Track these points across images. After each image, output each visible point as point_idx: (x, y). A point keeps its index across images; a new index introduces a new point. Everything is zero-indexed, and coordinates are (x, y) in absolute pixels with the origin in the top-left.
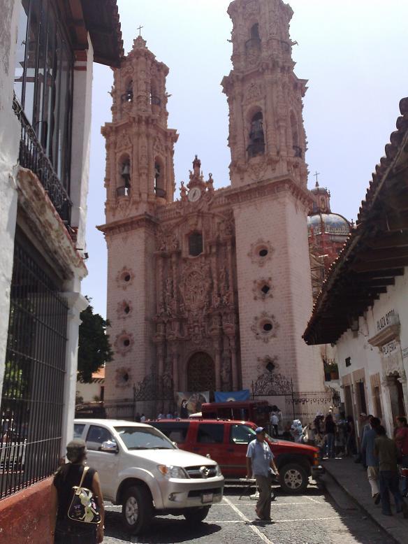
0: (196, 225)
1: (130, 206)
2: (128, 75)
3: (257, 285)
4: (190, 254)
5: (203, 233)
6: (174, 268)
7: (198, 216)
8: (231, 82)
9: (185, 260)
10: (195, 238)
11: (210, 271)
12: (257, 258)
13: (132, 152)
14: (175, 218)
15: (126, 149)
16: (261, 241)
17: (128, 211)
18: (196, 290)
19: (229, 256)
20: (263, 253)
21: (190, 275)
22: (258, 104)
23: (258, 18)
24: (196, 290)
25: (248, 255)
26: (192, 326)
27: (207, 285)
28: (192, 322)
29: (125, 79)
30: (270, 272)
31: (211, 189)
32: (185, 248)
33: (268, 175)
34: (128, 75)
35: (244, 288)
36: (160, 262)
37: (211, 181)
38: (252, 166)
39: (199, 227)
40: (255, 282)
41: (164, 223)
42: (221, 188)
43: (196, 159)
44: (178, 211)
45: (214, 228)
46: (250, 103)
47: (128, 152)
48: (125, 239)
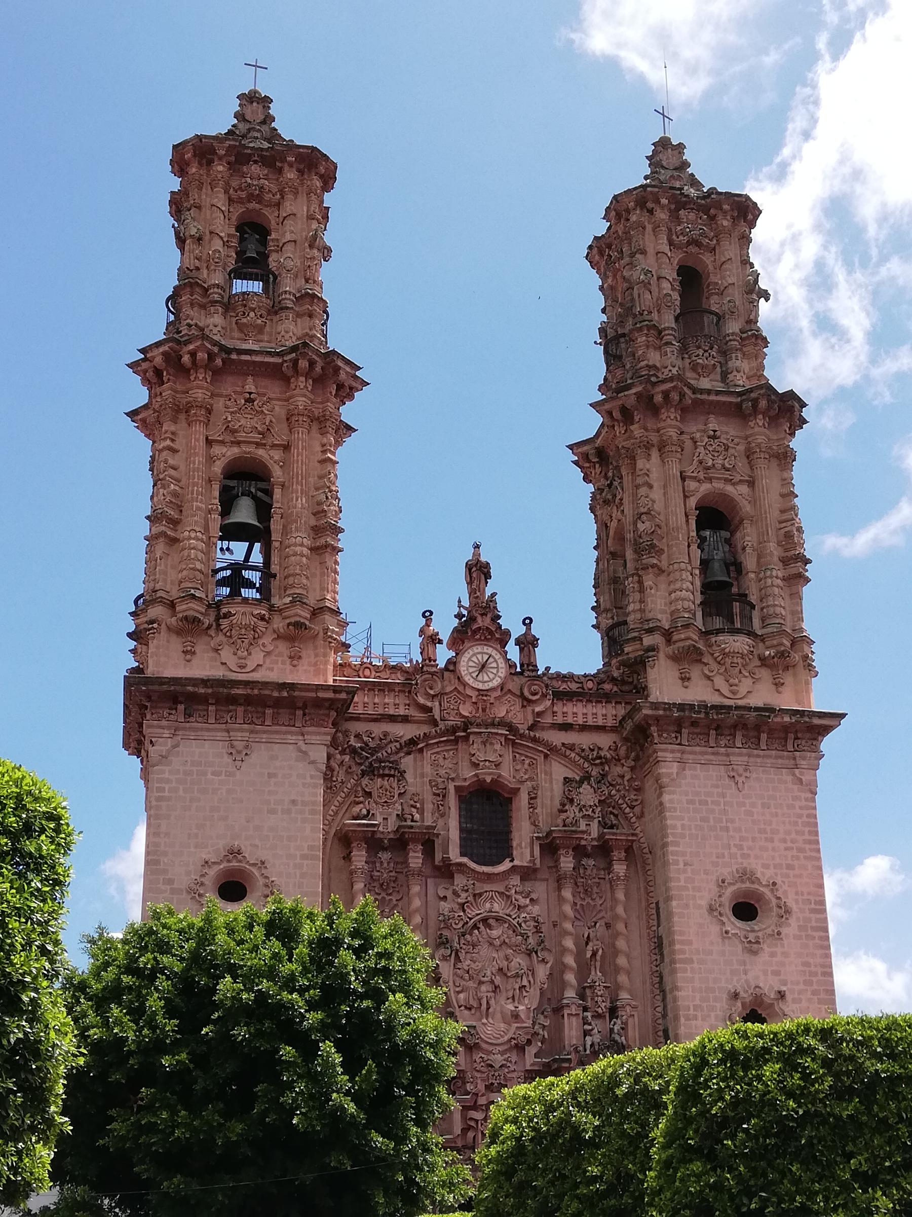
0: (497, 765)
1: (267, 640)
2: (253, 205)
3: (739, 1004)
4: (463, 854)
5: (523, 798)
6: (416, 889)
7: (506, 739)
8: (658, 398)
9: (446, 871)
10: (487, 810)
12: (763, 924)
13: (285, 465)
14: (405, 719)
15: (258, 445)
16: (746, 875)
17: (257, 657)
18: (498, 980)
19: (620, 896)
20: (745, 910)
21: (475, 927)
22: (729, 489)
23: (707, 258)
24: (498, 980)
25: (711, 909)
26: (482, 1101)
27: (542, 972)
28: (481, 1087)
29: (238, 211)
30: (776, 973)
31: (529, 665)
32: (451, 829)
33: (759, 693)
34: (253, 205)
35: (696, 1008)
36: (360, 857)
37: (528, 643)
38: (725, 654)
39: (507, 773)
40: (736, 996)
42: (564, 672)
43: (477, 555)
44: (421, 700)
45: (544, 793)
46: (710, 480)
47: (270, 457)
48: (239, 755)
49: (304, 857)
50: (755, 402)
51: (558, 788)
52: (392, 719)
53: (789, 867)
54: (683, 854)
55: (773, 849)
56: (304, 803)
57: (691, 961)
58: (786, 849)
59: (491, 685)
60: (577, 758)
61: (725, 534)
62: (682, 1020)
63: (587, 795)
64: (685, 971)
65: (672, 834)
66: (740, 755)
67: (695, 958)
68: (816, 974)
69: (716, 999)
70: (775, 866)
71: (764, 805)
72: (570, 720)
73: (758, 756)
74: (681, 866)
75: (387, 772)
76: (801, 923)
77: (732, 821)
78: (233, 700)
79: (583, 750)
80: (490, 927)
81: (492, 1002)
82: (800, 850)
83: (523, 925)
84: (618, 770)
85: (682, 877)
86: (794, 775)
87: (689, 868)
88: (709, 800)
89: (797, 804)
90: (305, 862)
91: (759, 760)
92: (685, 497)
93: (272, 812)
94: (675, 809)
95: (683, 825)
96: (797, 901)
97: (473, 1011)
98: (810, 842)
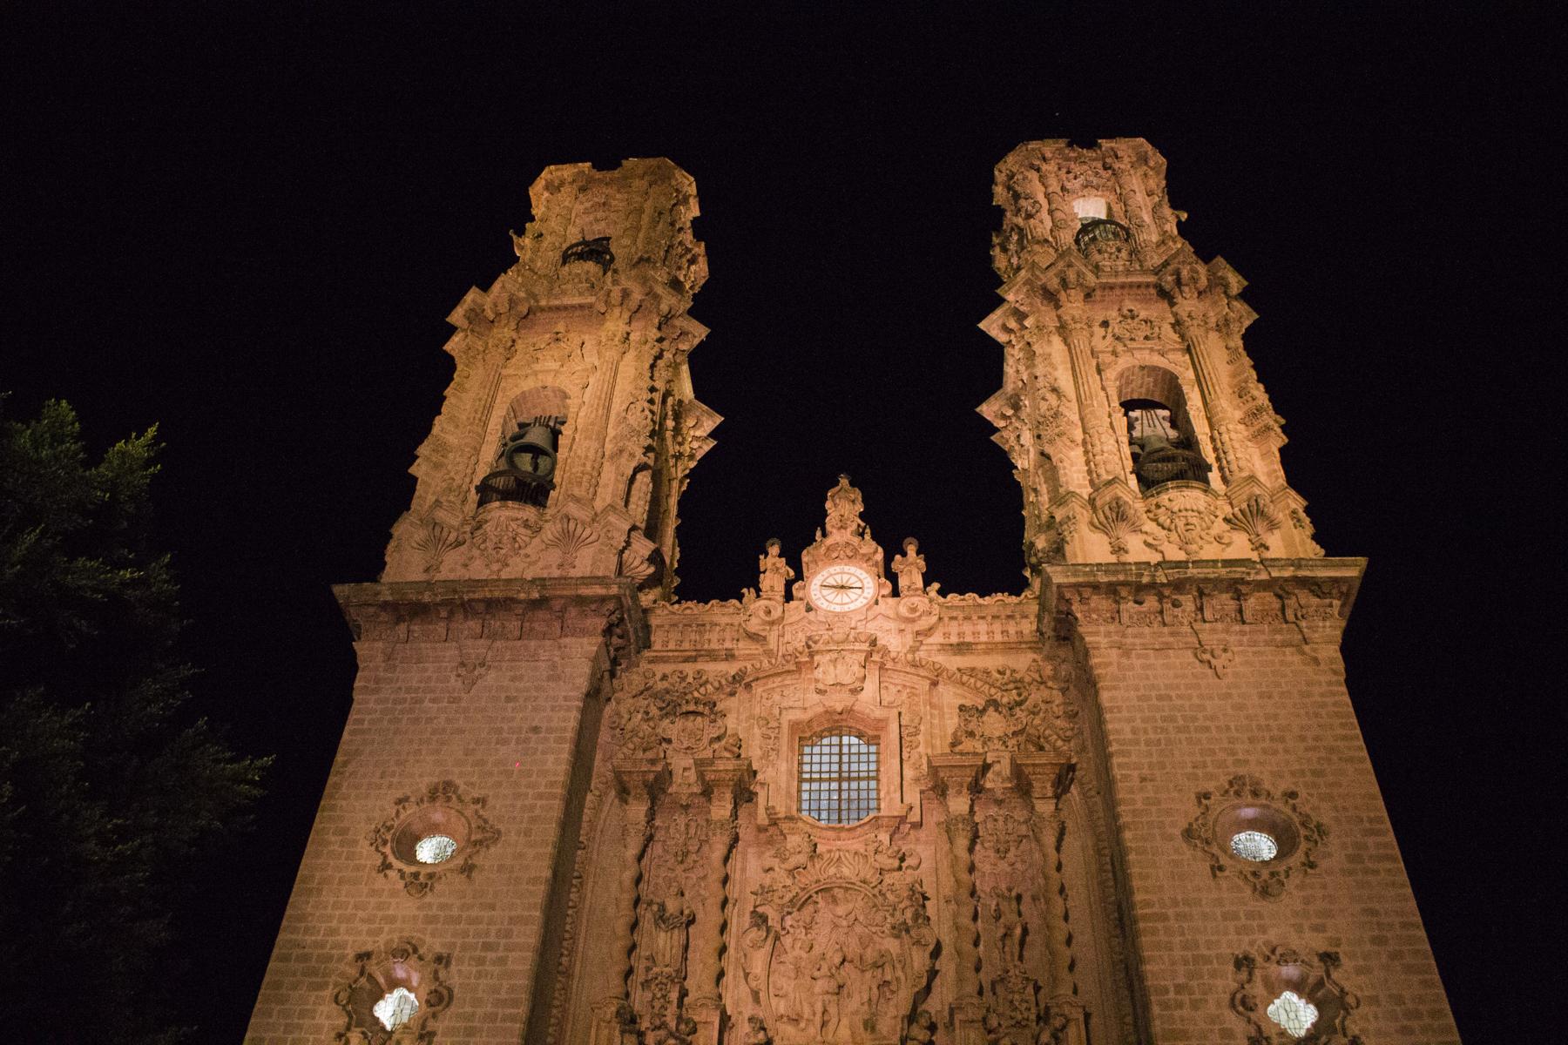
0: (854, 692)
11: (920, 899)
35: (1179, 989)
41: (668, 668)
49: (540, 796)
50: (1177, 273)
51: (952, 722)
52: (712, 656)
53: (1316, 773)
54: (1138, 767)
55: (1286, 751)
56: (550, 730)
57: (1165, 918)
58: (1306, 749)
59: (852, 607)
60: (979, 684)
61: (1166, 413)
62: (1156, 1010)
63: (994, 724)
64: (1154, 932)
65: (1117, 741)
66: (1213, 631)
67: (1171, 912)
68: (1391, 925)
69: (1213, 974)
70: (1293, 774)
71: (1261, 696)
72: (969, 639)
73: (1243, 633)
74: (1136, 783)
75: (692, 707)
76: (1350, 851)
77: (1213, 718)
78: (468, 608)
79: (988, 673)
80: (835, 900)
81: (833, 1010)
82: (1332, 750)
83: (889, 895)
84: (1045, 693)
85: (1138, 797)
86: (1303, 653)
87: (1149, 785)
88: (1173, 694)
89: (1316, 690)
90: (539, 803)
91: (1245, 639)
92: (1099, 371)
93: (505, 742)
94: (1119, 709)
95: (1134, 731)
96: (1337, 819)
97: (802, 1025)
98: (1345, 738)
